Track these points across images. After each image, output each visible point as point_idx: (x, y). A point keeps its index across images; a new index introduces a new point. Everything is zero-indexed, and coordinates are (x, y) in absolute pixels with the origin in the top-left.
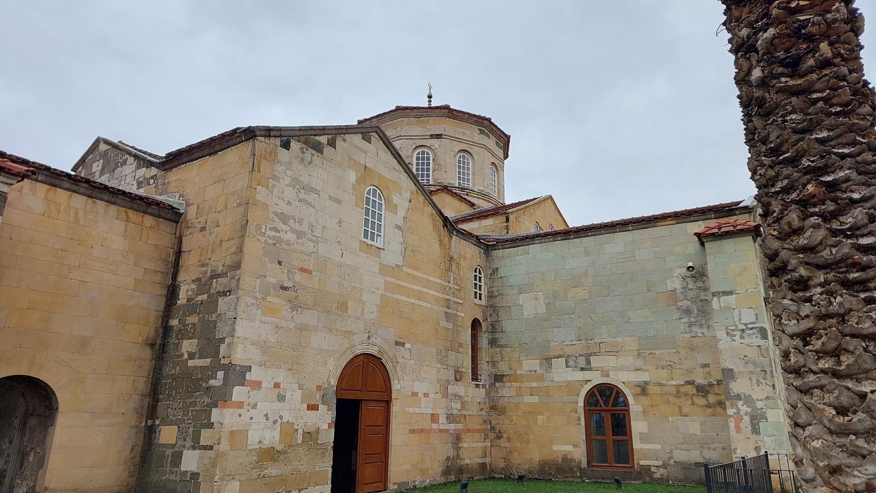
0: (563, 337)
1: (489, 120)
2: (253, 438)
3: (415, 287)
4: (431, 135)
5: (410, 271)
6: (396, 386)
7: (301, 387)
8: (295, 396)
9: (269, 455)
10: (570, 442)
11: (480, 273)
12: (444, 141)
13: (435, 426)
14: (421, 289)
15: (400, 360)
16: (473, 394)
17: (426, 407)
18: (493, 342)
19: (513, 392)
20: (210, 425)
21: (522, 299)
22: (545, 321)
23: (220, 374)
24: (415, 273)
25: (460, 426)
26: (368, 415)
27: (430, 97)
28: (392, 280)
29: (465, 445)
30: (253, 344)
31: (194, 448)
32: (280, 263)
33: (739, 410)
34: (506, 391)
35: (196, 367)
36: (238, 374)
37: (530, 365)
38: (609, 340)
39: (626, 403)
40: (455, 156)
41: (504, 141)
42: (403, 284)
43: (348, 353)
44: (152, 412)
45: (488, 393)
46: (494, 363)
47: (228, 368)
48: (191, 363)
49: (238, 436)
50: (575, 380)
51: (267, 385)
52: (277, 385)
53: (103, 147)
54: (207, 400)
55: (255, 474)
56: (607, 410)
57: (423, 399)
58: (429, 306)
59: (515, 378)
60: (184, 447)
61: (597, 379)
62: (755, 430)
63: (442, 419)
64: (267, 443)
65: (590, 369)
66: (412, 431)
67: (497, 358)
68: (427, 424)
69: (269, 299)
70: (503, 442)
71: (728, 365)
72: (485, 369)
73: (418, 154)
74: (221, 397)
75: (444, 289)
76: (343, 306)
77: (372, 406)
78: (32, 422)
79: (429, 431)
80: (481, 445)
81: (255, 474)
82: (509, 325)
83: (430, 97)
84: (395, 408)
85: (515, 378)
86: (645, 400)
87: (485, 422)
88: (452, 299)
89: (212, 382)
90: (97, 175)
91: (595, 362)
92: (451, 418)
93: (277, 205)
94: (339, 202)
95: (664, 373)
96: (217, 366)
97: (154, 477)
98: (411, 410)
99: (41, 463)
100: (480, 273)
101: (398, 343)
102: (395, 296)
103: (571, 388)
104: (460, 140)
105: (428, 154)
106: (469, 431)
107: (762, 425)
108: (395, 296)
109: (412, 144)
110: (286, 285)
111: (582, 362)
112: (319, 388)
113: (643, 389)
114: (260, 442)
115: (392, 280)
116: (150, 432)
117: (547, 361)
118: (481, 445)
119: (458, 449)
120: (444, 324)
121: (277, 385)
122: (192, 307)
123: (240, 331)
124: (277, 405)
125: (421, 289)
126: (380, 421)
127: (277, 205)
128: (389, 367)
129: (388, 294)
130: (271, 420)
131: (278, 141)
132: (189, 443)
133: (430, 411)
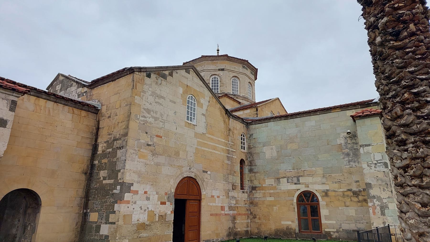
0: (285, 168)
1: (247, 61)
2: (135, 218)
3: (212, 144)
4: (219, 69)
5: (210, 136)
6: (203, 192)
7: (157, 193)
8: (154, 198)
9: (142, 226)
10: (290, 220)
11: (244, 137)
13: (223, 212)
14: (215, 145)
15: (205, 180)
16: (242, 196)
17: (218, 203)
18: (251, 171)
19: (261, 195)
20: (114, 212)
21: (265, 149)
22: (277, 160)
23: (118, 187)
24: (212, 137)
25: (235, 212)
26: (190, 207)
27: (218, 50)
28: (201, 140)
29: (238, 221)
30: (134, 172)
31: (106, 223)
32: (147, 133)
33: (374, 204)
34: (258, 195)
35: (107, 184)
36: (127, 187)
37: (269, 182)
38: (308, 169)
39: (318, 201)
40: (231, 79)
41: (255, 71)
42: (206, 142)
43: (180, 176)
44: (86, 206)
45: (249, 196)
46: (251, 181)
47: (122, 184)
48: (104, 182)
49: (127, 217)
51: (141, 192)
52: (146, 192)
53: (61, 78)
54: (112, 200)
55: (136, 236)
56: (308, 204)
57: (217, 199)
58: (219, 153)
60: (101, 223)
61: (303, 188)
62: (383, 214)
63: (227, 209)
64: (141, 221)
65: (299, 184)
66: (211, 215)
68: (219, 211)
69: (141, 150)
70: (257, 220)
71: (368, 181)
72: (247, 184)
73: (213, 78)
74: (119, 199)
75: (226, 145)
76: (177, 154)
77: (192, 202)
78: (29, 211)
79: (220, 215)
80: (246, 221)
81: (136, 236)
82: (259, 162)
83: (218, 50)
84: (203, 203)
86: (327, 199)
87: (247, 210)
88: (230, 149)
89: (115, 191)
90: (59, 91)
91: (302, 180)
92: (231, 208)
93: (145, 105)
94: (175, 103)
95: (336, 186)
96: (117, 183)
97: (87, 238)
98: (211, 204)
99: (34, 230)
100: (244, 137)
101: (204, 171)
102: (203, 148)
103: (290, 193)
104: (233, 71)
105: (217, 78)
106: (240, 214)
108: (203, 148)
109: (210, 73)
110: (149, 143)
111: (295, 180)
112: (166, 194)
113: (326, 193)
114: (138, 220)
115: (201, 140)
116: (85, 216)
117: (278, 179)
118: (246, 221)
119: (234, 223)
120: (226, 162)
121: (146, 192)
122: (105, 155)
123: (127, 167)
124: (146, 202)
125: (215, 145)
126: (196, 210)
127: (145, 105)
128: (200, 183)
129: (199, 147)
130: (143, 210)
131: (145, 74)
132: (104, 221)
133: (220, 205)
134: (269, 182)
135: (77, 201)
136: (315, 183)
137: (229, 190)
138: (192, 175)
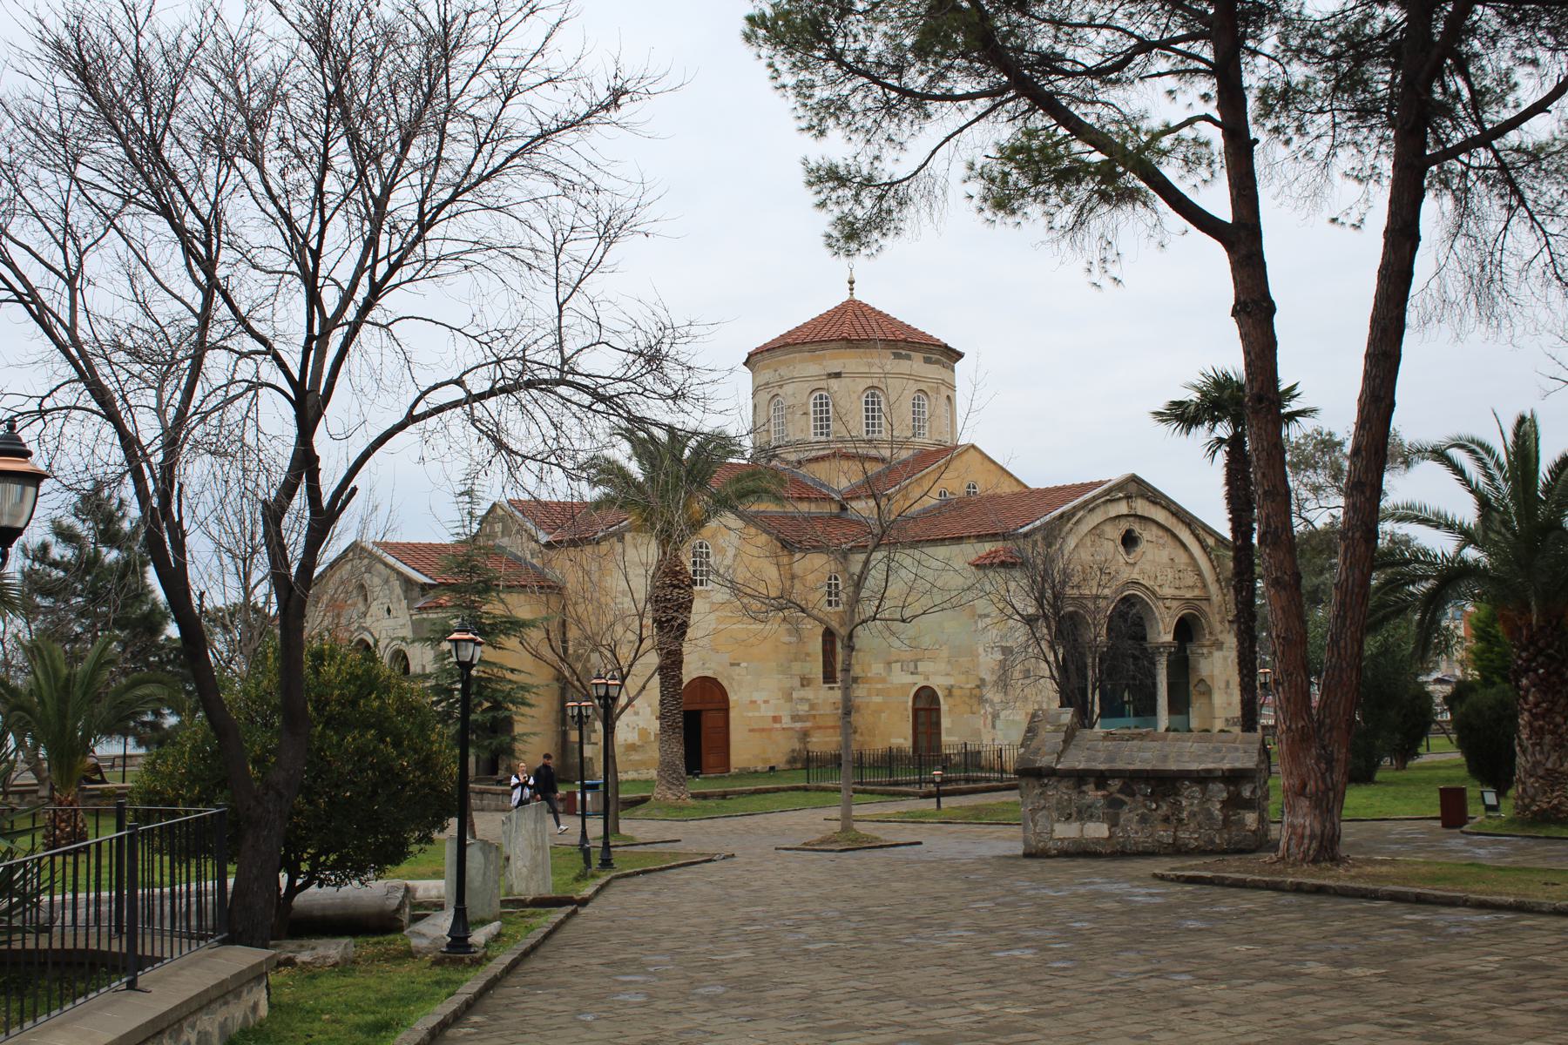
6: (732, 697)
10: (902, 738)
12: (844, 381)
16: (827, 697)
17: (767, 712)
25: (808, 724)
26: (709, 721)
50: (905, 681)
56: (926, 707)
64: (630, 741)
66: (751, 731)
68: (769, 724)
84: (732, 714)
85: (866, 680)
91: (921, 667)
95: (963, 678)
103: (904, 688)
104: (864, 375)
107: (998, 722)
109: (808, 387)
111: (912, 665)
113: (950, 692)
116: (564, 734)
117: (889, 664)
119: (806, 743)
128: (725, 683)
134: (877, 668)
135: (553, 716)
136: (934, 674)
137: (793, 689)
138: (709, 674)
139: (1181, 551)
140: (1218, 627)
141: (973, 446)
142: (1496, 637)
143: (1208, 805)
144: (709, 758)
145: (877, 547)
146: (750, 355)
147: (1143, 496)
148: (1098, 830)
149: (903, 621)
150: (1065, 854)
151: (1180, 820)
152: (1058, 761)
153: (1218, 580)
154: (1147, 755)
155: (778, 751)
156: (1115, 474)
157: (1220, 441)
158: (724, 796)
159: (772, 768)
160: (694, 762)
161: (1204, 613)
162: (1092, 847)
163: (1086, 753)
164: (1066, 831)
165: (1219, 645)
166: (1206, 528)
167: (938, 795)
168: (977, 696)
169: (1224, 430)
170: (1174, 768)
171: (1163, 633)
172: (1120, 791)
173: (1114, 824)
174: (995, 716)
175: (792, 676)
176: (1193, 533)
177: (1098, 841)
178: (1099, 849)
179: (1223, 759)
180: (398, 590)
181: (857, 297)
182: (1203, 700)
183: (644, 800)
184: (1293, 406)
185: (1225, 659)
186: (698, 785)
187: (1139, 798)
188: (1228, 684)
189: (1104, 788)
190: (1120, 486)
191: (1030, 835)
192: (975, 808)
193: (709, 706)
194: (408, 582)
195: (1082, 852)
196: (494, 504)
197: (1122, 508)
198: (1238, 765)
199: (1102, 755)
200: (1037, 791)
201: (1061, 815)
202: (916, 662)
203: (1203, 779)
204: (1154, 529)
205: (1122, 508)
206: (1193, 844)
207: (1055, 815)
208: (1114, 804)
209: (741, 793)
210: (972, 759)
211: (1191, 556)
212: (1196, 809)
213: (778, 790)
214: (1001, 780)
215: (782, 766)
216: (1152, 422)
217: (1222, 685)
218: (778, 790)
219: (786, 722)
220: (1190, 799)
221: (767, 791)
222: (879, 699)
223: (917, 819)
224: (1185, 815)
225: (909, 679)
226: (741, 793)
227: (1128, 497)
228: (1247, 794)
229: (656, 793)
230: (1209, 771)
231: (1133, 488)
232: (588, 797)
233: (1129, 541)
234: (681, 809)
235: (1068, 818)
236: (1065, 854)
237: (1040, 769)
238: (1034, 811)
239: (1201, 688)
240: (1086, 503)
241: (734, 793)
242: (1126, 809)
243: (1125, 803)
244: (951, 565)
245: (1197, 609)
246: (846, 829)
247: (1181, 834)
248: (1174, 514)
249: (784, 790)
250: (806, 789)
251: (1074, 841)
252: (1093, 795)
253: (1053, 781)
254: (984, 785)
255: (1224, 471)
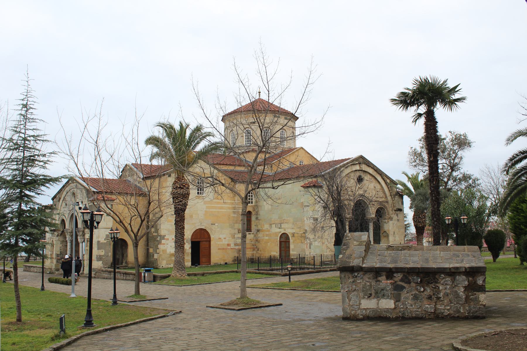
0: (275, 217)
6: (212, 237)
10: (275, 252)
13: (229, 247)
18: (257, 218)
19: (262, 236)
26: (203, 245)
34: (260, 235)
36: (163, 237)
37: (266, 226)
44: (148, 245)
45: (255, 236)
46: (256, 225)
47: (160, 236)
49: (164, 251)
50: (277, 231)
55: (169, 259)
56: (285, 241)
57: (224, 240)
59: (263, 231)
62: (310, 248)
66: (219, 249)
67: (258, 224)
68: (226, 247)
70: (259, 252)
72: (253, 227)
74: (160, 242)
77: (204, 243)
78: (124, 247)
79: (226, 249)
81: (169, 259)
82: (261, 213)
84: (212, 243)
85: (263, 231)
87: (253, 245)
91: (283, 226)
96: (158, 235)
97: (150, 260)
99: (127, 256)
101: (212, 224)
103: (276, 234)
107: (312, 247)
111: (279, 225)
116: (148, 249)
117: (271, 225)
123: (162, 227)
126: (207, 246)
128: (209, 231)
129: (208, 210)
134: (266, 226)
136: (288, 228)
139: (378, 184)
140: (391, 212)
141: (302, 148)
142: (522, 210)
143: (456, 289)
144: (203, 259)
145: (261, 152)
146: (224, 116)
147: (364, 163)
148: (388, 304)
149: (273, 188)
150: (367, 318)
151: (438, 298)
152: (363, 263)
153: (391, 195)
154: (416, 259)
155: (229, 257)
156: (353, 155)
157: (420, 115)
158: (203, 275)
159: (226, 263)
160: (196, 260)
161: (386, 208)
162: (384, 314)
163: (378, 257)
164: (369, 304)
165: (391, 219)
166: (386, 176)
167: (290, 275)
168: (304, 236)
169: (423, 109)
170: (434, 266)
171: (372, 212)
172: (402, 280)
173: (397, 300)
174: (311, 244)
175: (235, 229)
176: (382, 178)
177: (387, 310)
178: (388, 315)
179: (462, 261)
180: (85, 194)
181: (261, 98)
182: (385, 239)
183: (169, 276)
184: (456, 96)
185: (393, 224)
186: (197, 270)
187: (413, 284)
188: (394, 233)
189: (391, 279)
190: (357, 159)
191: (346, 306)
192: (305, 281)
193: (203, 240)
194: (88, 191)
195: (378, 317)
196: (126, 165)
197: (357, 167)
198: (474, 265)
199: (389, 259)
200: (351, 280)
201: (365, 295)
202: (281, 224)
203: (453, 273)
204: (369, 176)
205: (357, 167)
206: (446, 313)
207: (361, 294)
208: (398, 288)
209: (210, 274)
210: (302, 260)
211: (381, 186)
212: (448, 291)
213: (225, 272)
214: (314, 268)
215: (231, 262)
216: (390, 104)
217: (392, 233)
218: (225, 272)
219: (232, 246)
220: (444, 285)
221: (221, 273)
222: (267, 238)
223: (279, 287)
224: (441, 295)
225: (279, 230)
226: (210, 274)
227: (360, 164)
228: (480, 282)
229: (173, 273)
230: (457, 268)
231: (361, 160)
232: (146, 274)
233: (360, 180)
234: (182, 280)
235: (370, 296)
236: (367, 318)
237: (353, 267)
238: (349, 292)
239: (385, 234)
240: (344, 165)
241: (207, 273)
242: (405, 291)
243: (405, 288)
244: (293, 189)
245: (384, 206)
246: (243, 296)
247: (438, 306)
248: (375, 170)
249: (228, 272)
250: (237, 272)
251: (373, 310)
252: (385, 282)
253: (361, 273)
254: (306, 271)
255: (424, 126)
